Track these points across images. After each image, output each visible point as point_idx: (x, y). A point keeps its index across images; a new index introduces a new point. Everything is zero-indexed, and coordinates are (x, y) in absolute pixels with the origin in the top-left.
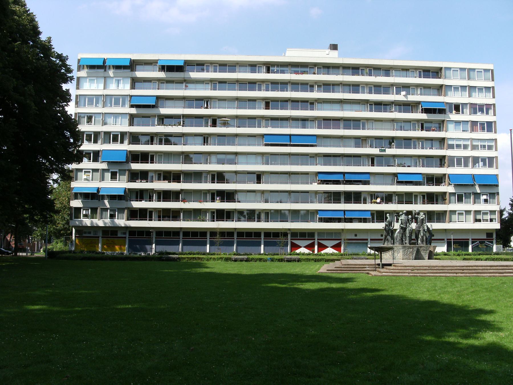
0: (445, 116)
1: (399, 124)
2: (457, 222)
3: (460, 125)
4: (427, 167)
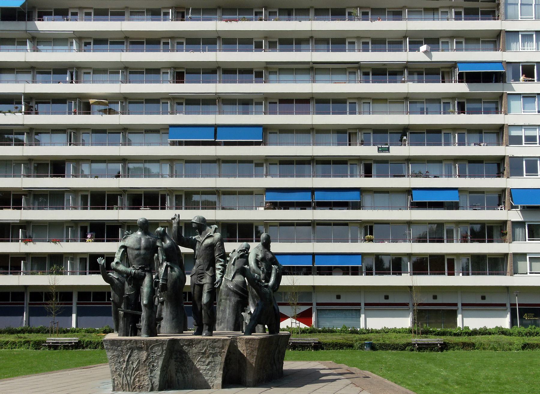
0: (503, 86)
1: (419, 106)
3: (535, 101)
4: (470, 176)
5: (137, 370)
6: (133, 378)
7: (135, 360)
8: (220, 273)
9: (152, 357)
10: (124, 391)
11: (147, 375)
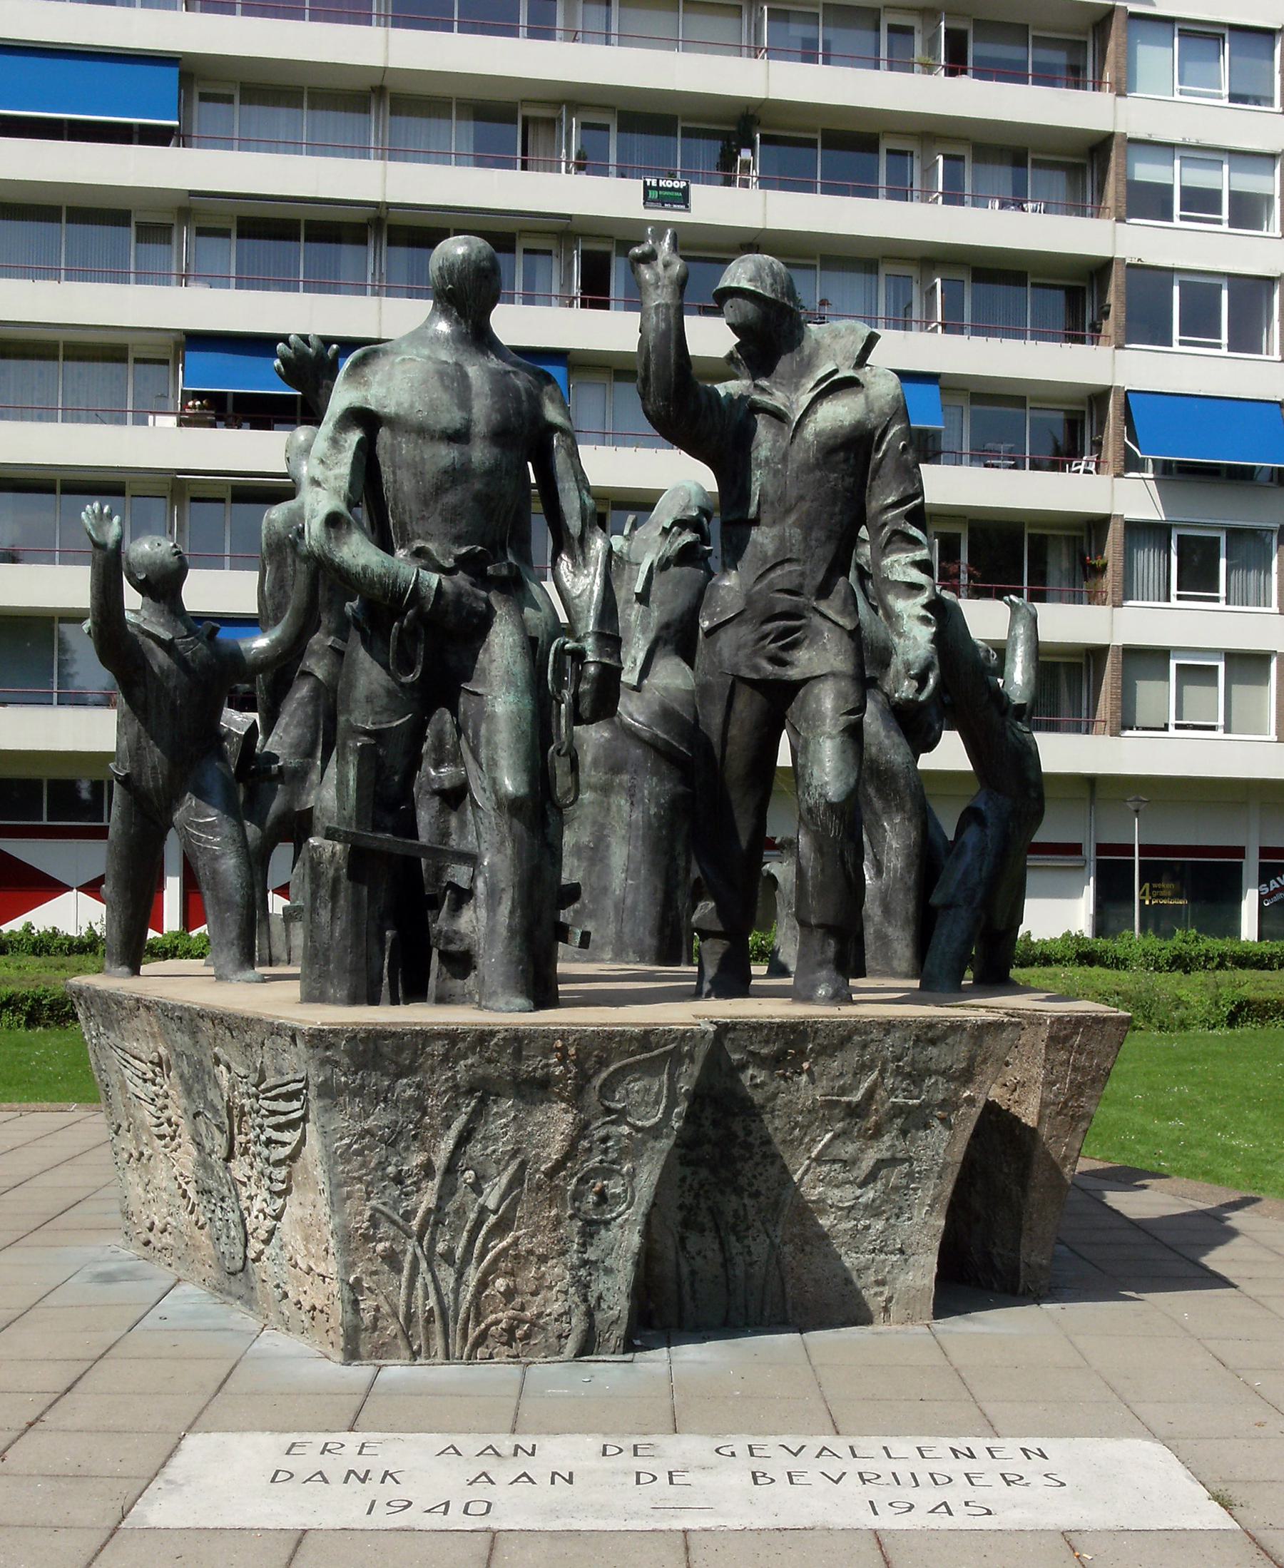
2: (1173, 732)
4: (977, 331)
5: (502, 1227)
6: (473, 1275)
7: (498, 1162)
8: (923, 612)
9: (605, 1140)
10: (415, 1355)
11: (563, 1253)
